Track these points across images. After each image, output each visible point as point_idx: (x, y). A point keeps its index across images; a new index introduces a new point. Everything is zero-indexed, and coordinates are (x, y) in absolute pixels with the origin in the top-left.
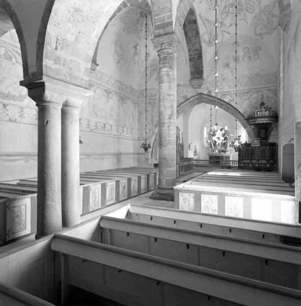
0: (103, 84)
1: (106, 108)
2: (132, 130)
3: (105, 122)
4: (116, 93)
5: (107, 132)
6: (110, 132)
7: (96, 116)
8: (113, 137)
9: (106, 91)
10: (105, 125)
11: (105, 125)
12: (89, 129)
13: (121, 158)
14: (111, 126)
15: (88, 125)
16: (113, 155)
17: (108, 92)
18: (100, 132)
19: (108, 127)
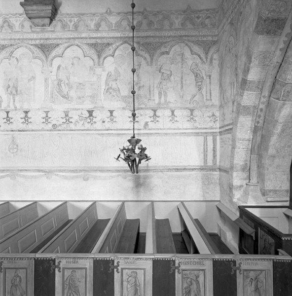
0: (83, 35)
1: (95, 79)
2: (192, 111)
3: (90, 107)
4: (125, 40)
5: (98, 125)
6: (107, 125)
7: (65, 100)
8: (119, 134)
9: (94, 46)
10: (90, 113)
11: (90, 113)
12: (50, 126)
13: (146, 178)
14: (111, 112)
15: (47, 119)
16: (118, 171)
17: (100, 49)
18: (79, 126)
19: (99, 115)
